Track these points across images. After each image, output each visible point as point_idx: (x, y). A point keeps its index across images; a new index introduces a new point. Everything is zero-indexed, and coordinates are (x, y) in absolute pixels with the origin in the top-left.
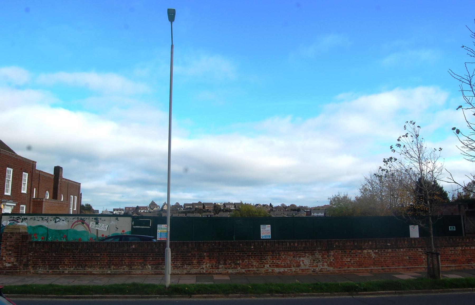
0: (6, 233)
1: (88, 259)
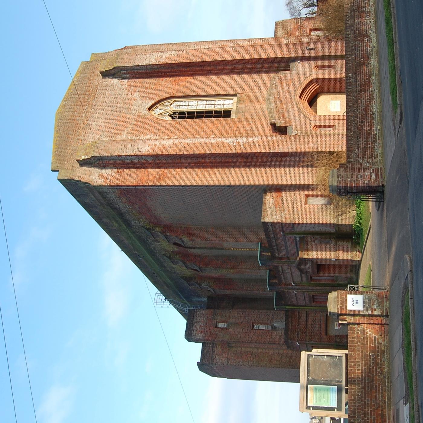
0: (337, 182)
1: (364, 109)
